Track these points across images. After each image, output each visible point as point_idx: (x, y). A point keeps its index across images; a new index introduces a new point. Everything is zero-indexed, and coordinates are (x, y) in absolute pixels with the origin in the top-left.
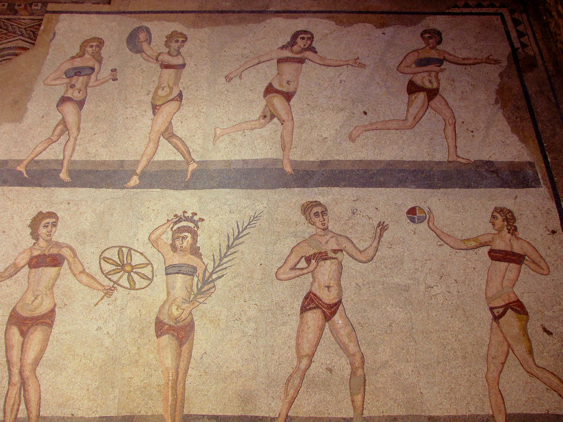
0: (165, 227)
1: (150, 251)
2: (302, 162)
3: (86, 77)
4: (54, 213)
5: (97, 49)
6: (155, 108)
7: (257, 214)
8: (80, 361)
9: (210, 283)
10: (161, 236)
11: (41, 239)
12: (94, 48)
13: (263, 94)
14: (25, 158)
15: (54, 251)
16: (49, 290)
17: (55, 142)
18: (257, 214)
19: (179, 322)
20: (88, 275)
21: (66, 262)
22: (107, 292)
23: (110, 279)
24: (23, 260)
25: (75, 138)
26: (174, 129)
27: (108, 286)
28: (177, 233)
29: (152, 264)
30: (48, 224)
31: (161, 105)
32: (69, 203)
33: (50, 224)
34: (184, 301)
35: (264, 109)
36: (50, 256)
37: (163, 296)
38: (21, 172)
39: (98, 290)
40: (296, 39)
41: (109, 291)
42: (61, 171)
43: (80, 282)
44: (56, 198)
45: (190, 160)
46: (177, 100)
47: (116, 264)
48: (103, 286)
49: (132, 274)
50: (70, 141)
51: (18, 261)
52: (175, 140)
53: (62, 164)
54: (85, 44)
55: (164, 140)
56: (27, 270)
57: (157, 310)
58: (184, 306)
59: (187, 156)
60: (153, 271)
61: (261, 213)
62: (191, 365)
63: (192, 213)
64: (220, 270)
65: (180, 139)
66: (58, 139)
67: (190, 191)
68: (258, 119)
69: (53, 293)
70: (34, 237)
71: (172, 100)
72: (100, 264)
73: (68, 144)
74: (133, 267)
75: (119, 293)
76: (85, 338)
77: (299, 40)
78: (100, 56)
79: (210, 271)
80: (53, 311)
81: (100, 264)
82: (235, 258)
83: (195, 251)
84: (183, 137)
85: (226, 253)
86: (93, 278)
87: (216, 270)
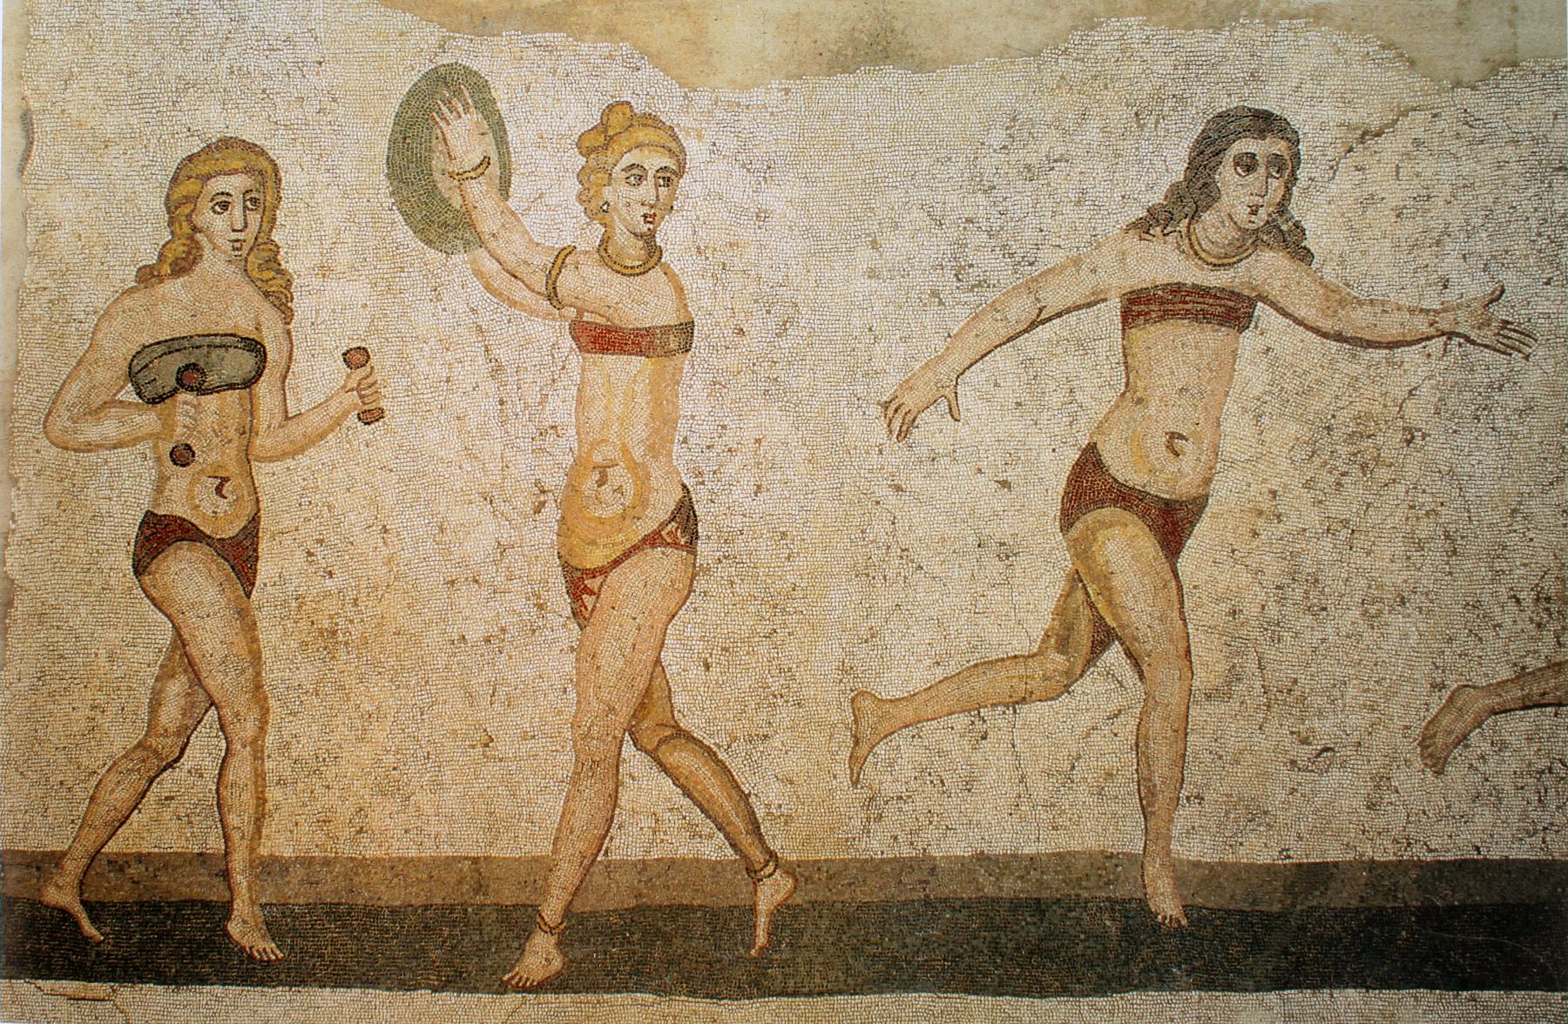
3: (232, 396)
5: (254, 218)
6: (579, 584)
12: (237, 211)
13: (1055, 510)
17: (170, 765)
25: (254, 741)
31: (603, 571)
35: (1068, 595)
38: (65, 914)
40: (1214, 169)
45: (757, 856)
46: (676, 545)
50: (234, 762)
52: (682, 758)
53: (226, 875)
54: (190, 187)
55: (639, 755)
59: (746, 840)
68: (1041, 652)
71: (653, 540)
73: (230, 777)
77: (1227, 175)
78: (272, 262)
84: (719, 746)
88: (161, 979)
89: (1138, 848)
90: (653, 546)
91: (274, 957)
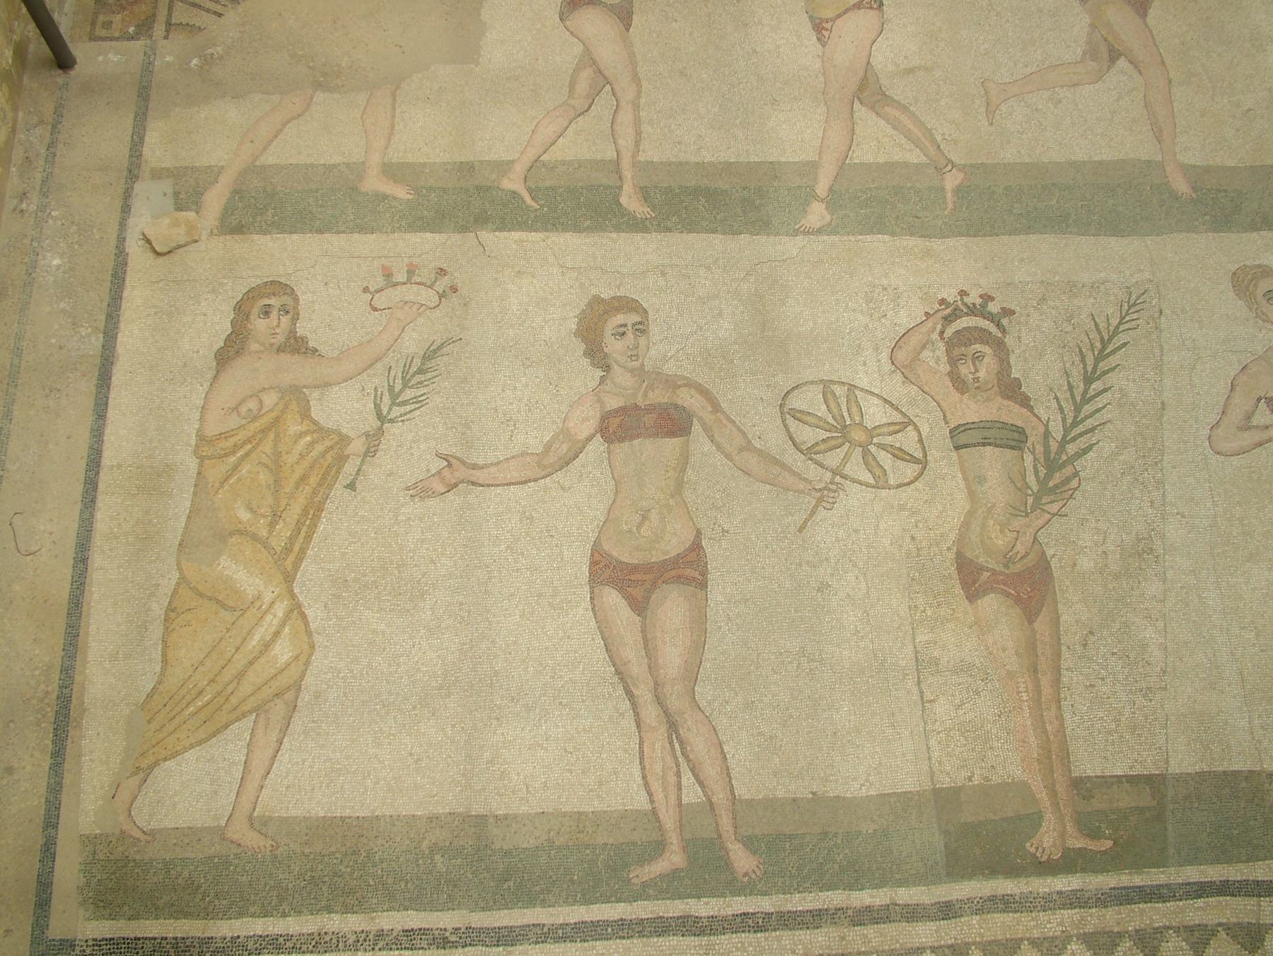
0: (924, 329)
1: (897, 389)
2: (1207, 170)
4: (633, 300)
6: (819, 27)
7: (1134, 297)
8: (798, 667)
9: (1063, 465)
10: (919, 353)
11: (616, 367)
14: (517, 155)
15: (659, 396)
16: (672, 496)
18: (1134, 297)
19: (1014, 563)
20: (764, 455)
21: (696, 427)
22: (822, 497)
23: (822, 466)
24: (584, 423)
26: (882, 81)
27: (820, 480)
28: (957, 345)
29: (915, 425)
30: (623, 329)
32: (663, 274)
33: (630, 328)
34: (1013, 512)
36: (650, 409)
37: (961, 503)
39: (797, 491)
41: (826, 492)
42: (621, 188)
43: (747, 474)
44: (626, 261)
46: (871, 8)
47: (827, 427)
48: (806, 480)
49: (873, 449)
51: (571, 424)
53: (618, 171)
56: (602, 448)
57: (953, 536)
58: (1017, 523)
59: (932, 151)
60: (921, 441)
61: (1143, 294)
62: (1064, 665)
63: (981, 296)
64: (1081, 435)
65: (904, 108)
66: (590, 107)
67: (963, 240)
69: (685, 502)
70: (596, 362)
72: (785, 426)
74: (871, 432)
75: (853, 498)
76: (796, 611)
79: (1058, 435)
80: (696, 547)
81: (785, 426)
82: (1109, 404)
83: (1012, 390)
84: (911, 105)
85: (1086, 391)
86: (777, 462)
87: (1073, 435)
88: (577, 229)
89: (1159, 158)
90: (859, 8)
91: (649, 216)
